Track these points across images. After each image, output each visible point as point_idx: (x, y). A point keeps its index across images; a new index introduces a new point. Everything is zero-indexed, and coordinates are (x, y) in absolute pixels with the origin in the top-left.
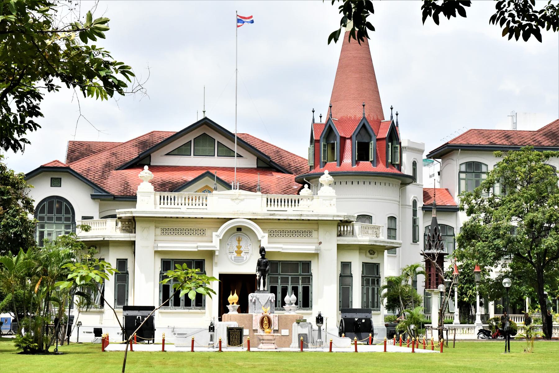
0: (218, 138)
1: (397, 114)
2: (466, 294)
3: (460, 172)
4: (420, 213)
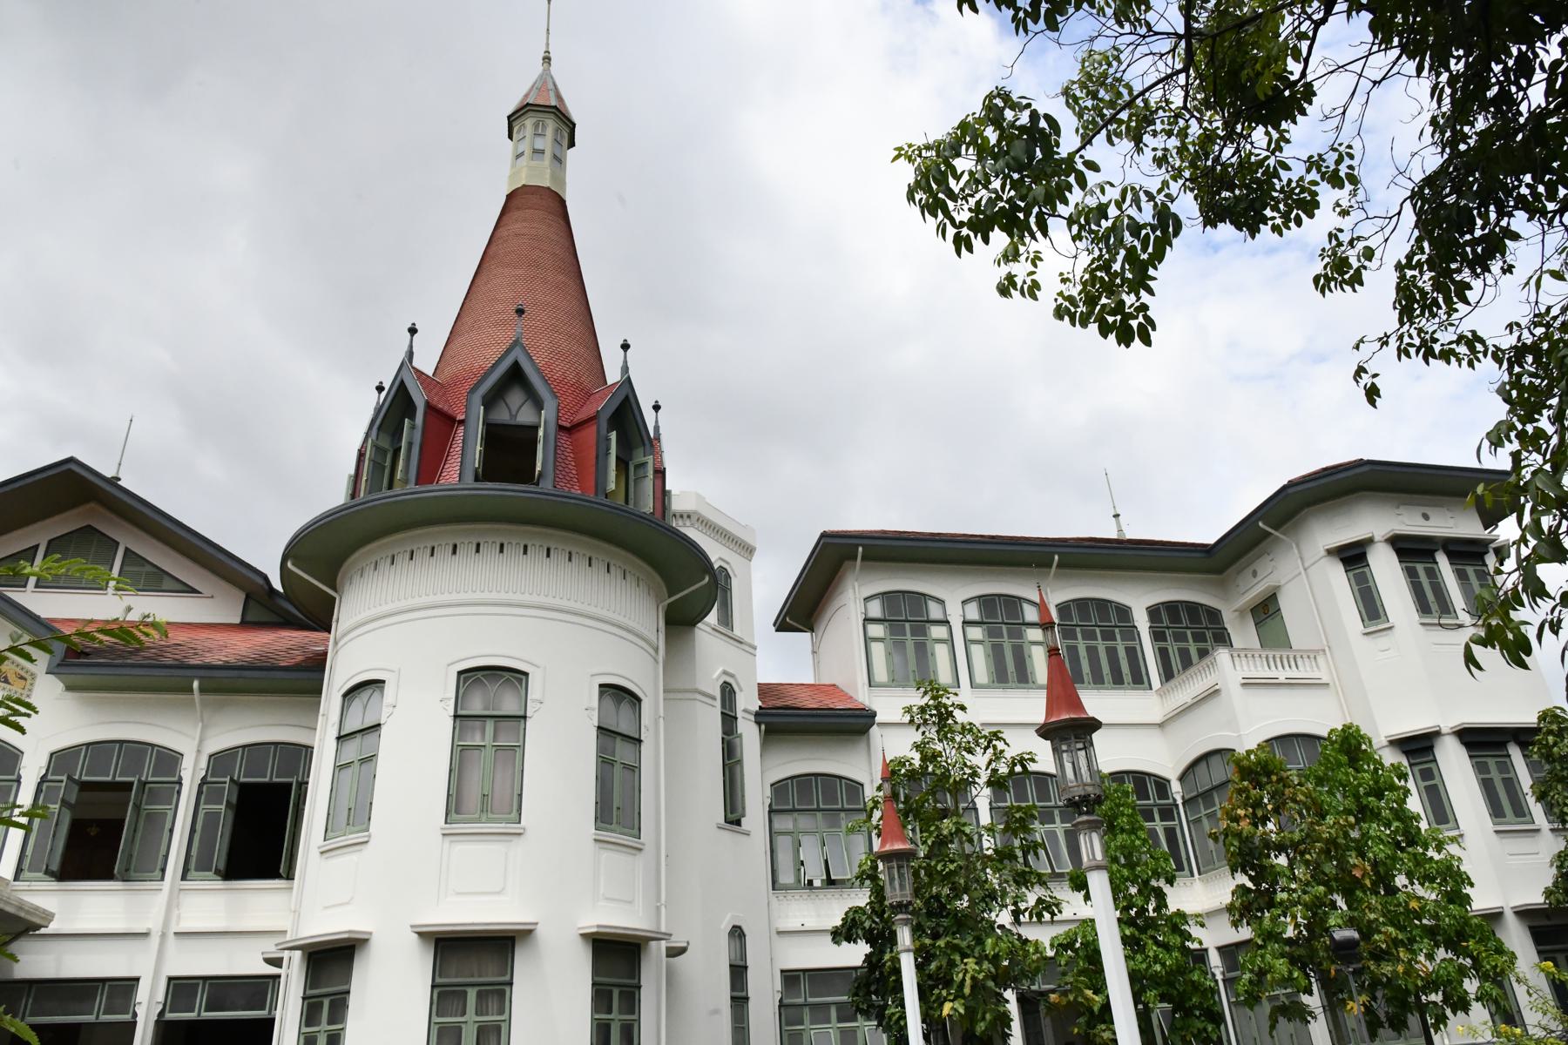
0: (127, 539)
1: (657, 408)
2: (948, 983)
3: (868, 620)
4: (749, 733)
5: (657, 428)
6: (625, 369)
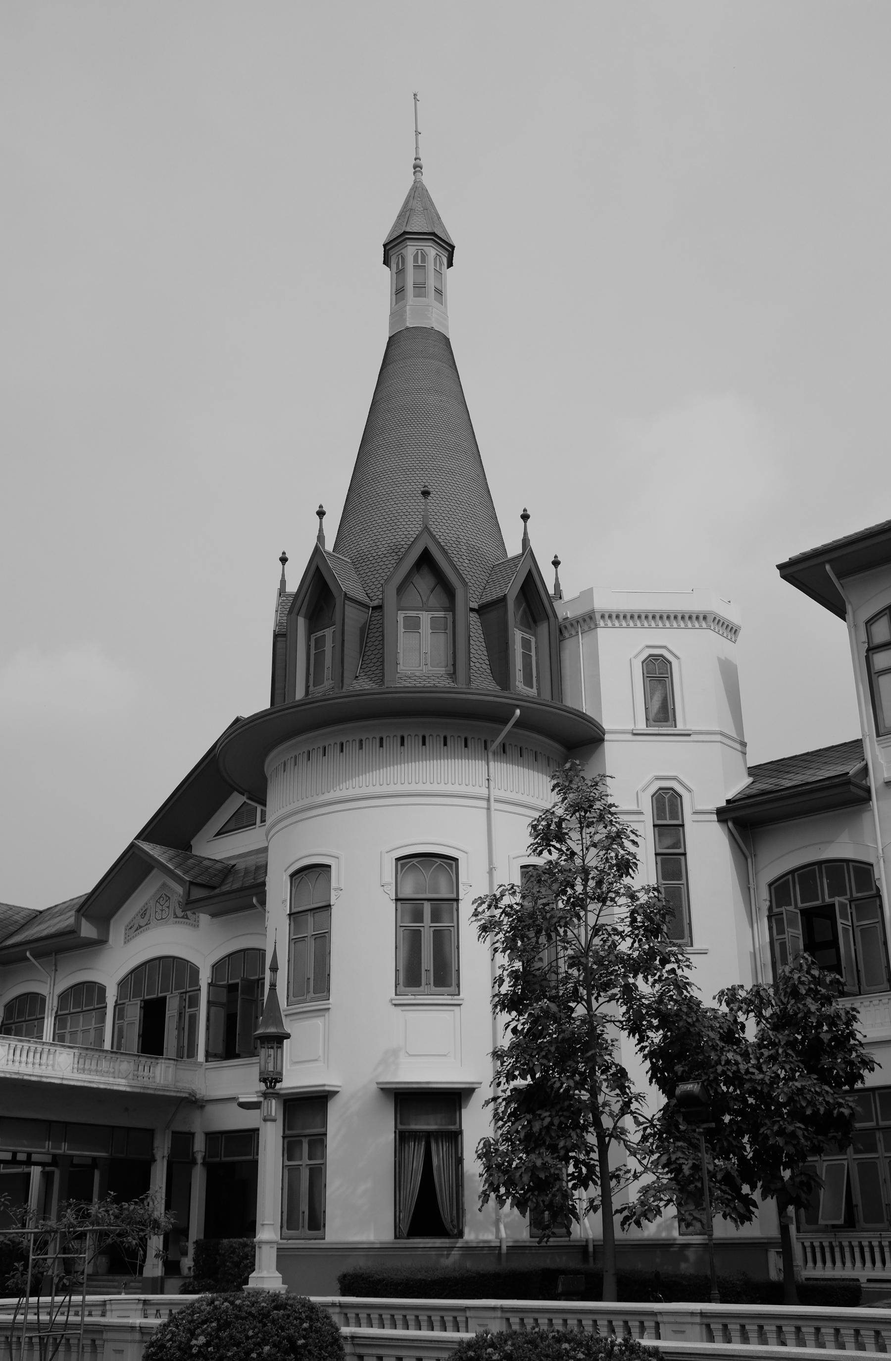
1: (556, 563)
5: (557, 586)
6: (525, 542)
